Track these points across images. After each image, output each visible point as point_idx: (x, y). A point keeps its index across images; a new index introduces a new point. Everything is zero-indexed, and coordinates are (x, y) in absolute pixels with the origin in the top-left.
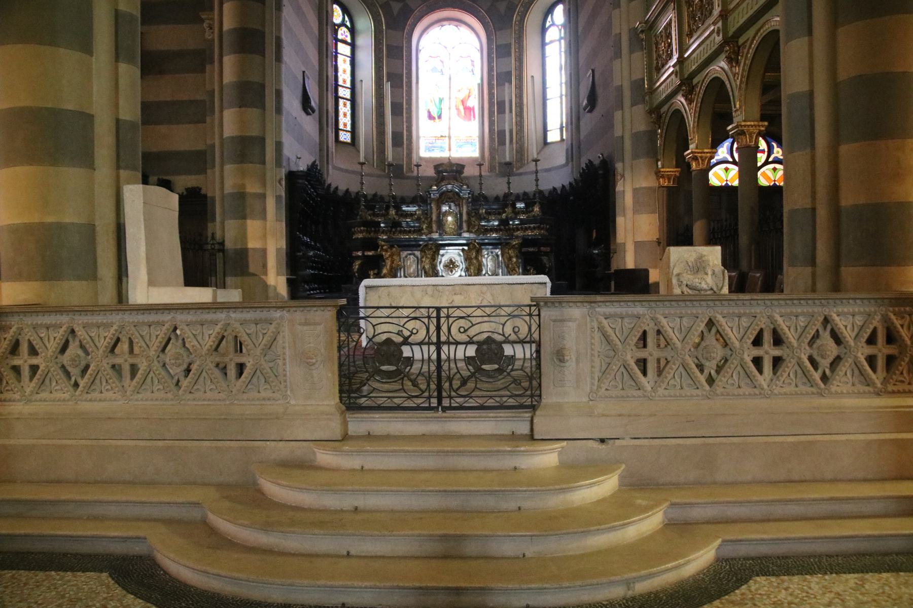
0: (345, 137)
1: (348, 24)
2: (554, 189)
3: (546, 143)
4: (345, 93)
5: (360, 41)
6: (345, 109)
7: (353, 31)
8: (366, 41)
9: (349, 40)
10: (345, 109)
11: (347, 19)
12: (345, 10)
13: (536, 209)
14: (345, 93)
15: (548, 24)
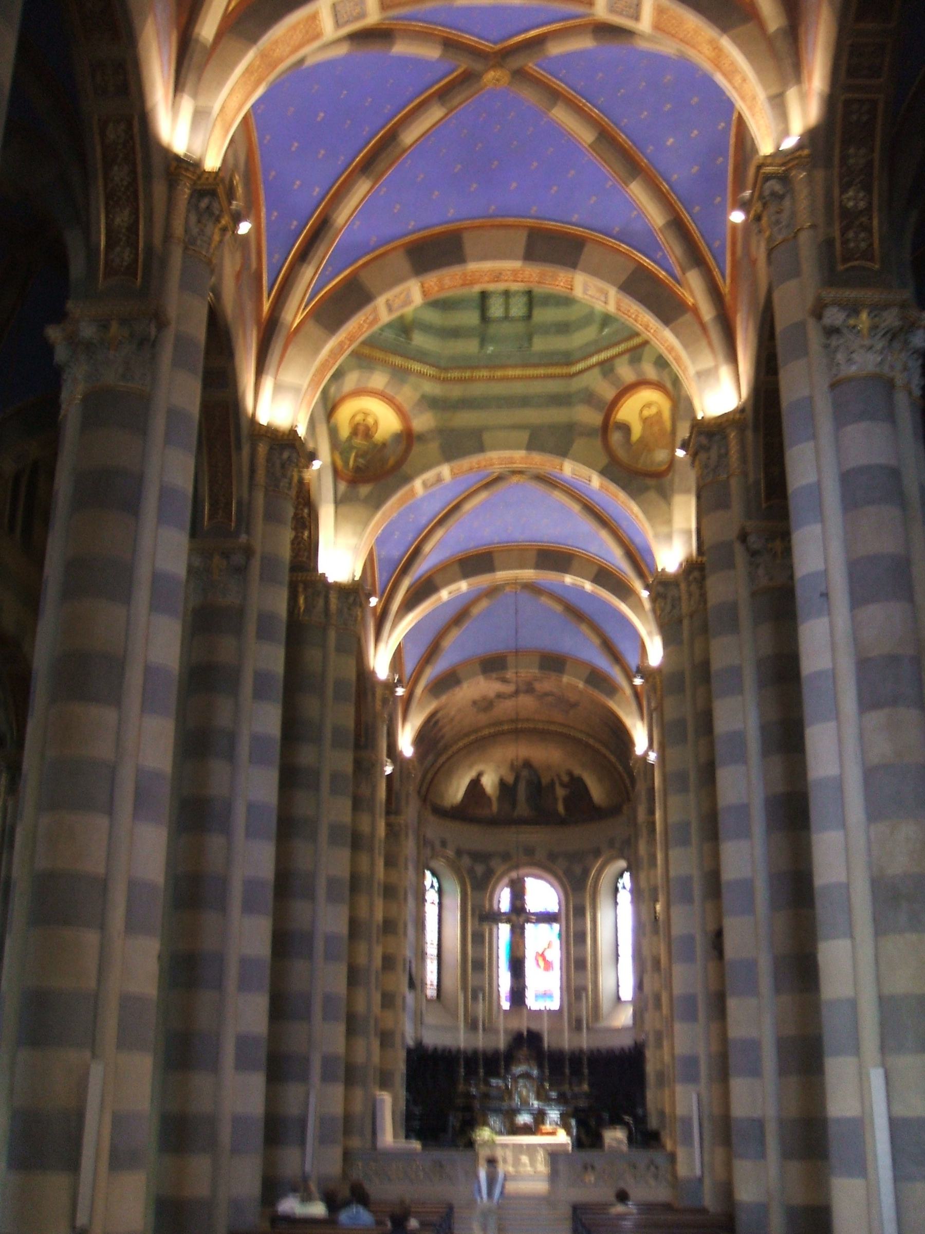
0: (431, 992)
1: (436, 885)
2: (622, 1049)
3: (619, 998)
4: (431, 950)
5: (447, 901)
6: (431, 968)
7: (440, 892)
8: (454, 902)
9: (437, 901)
10: (431, 968)
11: (435, 880)
12: (434, 874)
13: (585, 1087)
14: (431, 950)
15: (620, 886)
